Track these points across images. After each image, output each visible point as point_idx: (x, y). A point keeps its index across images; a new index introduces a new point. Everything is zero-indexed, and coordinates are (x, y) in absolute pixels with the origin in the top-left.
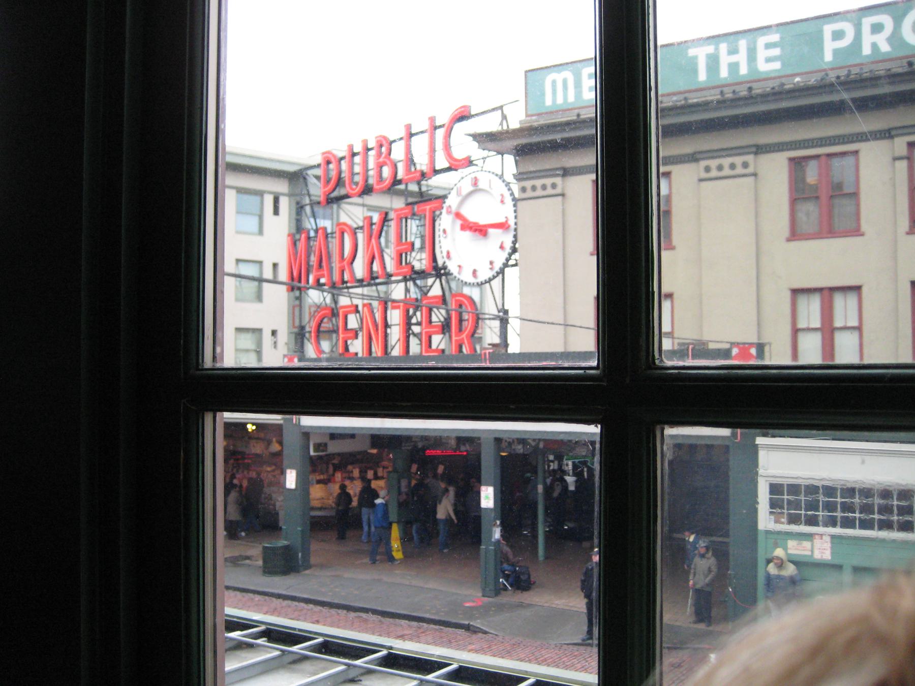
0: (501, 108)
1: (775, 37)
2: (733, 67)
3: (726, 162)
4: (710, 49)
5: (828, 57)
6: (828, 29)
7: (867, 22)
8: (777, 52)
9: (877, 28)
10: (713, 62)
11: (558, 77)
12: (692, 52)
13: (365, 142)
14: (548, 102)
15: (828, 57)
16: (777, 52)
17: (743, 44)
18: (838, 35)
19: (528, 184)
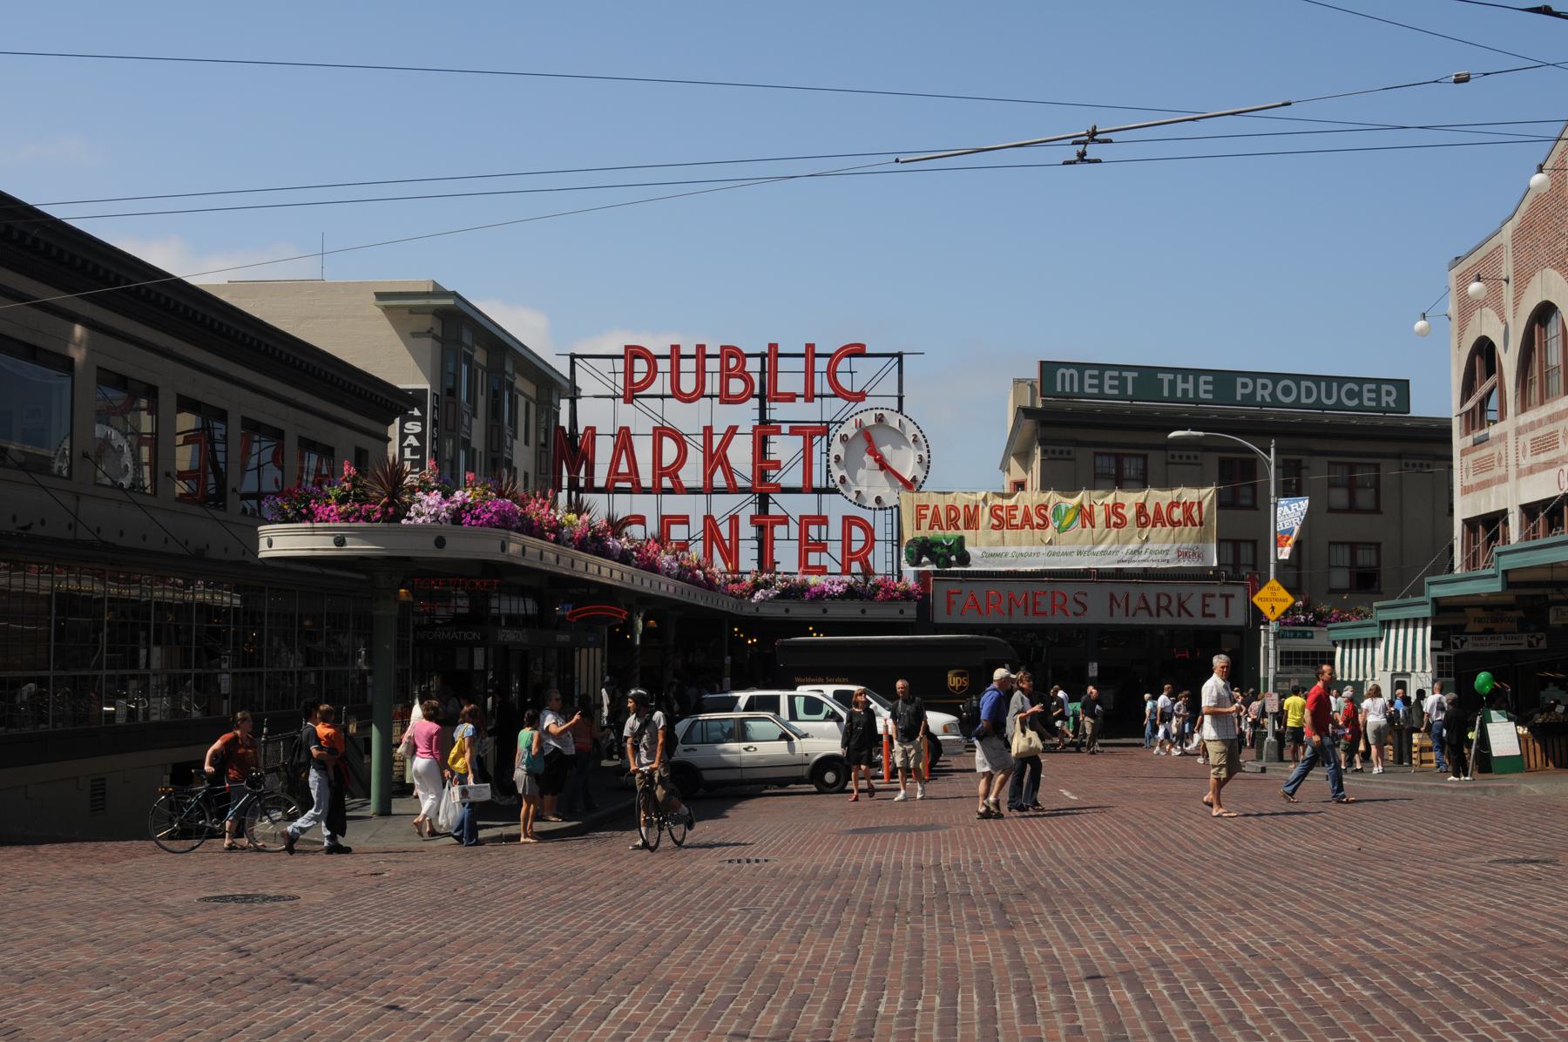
0: (900, 356)
1: (1210, 378)
2: (1185, 391)
3: (1185, 454)
4: (1171, 376)
5: (1239, 398)
6: (1240, 380)
7: (1260, 381)
8: (1210, 387)
9: (1264, 387)
10: (1173, 384)
11: (1068, 372)
12: (1160, 376)
13: (701, 348)
14: (1059, 389)
15: (1239, 398)
16: (1210, 387)
17: (1191, 378)
18: (1245, 386)
19: (1050, 448)
